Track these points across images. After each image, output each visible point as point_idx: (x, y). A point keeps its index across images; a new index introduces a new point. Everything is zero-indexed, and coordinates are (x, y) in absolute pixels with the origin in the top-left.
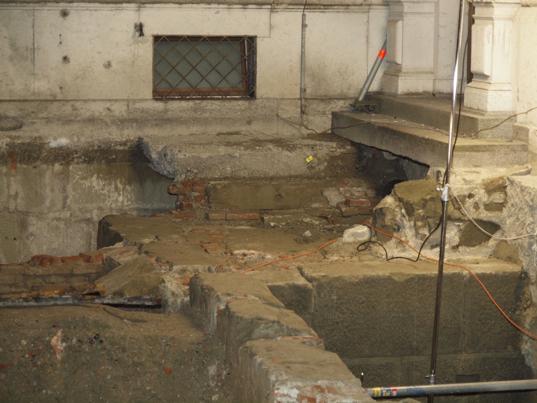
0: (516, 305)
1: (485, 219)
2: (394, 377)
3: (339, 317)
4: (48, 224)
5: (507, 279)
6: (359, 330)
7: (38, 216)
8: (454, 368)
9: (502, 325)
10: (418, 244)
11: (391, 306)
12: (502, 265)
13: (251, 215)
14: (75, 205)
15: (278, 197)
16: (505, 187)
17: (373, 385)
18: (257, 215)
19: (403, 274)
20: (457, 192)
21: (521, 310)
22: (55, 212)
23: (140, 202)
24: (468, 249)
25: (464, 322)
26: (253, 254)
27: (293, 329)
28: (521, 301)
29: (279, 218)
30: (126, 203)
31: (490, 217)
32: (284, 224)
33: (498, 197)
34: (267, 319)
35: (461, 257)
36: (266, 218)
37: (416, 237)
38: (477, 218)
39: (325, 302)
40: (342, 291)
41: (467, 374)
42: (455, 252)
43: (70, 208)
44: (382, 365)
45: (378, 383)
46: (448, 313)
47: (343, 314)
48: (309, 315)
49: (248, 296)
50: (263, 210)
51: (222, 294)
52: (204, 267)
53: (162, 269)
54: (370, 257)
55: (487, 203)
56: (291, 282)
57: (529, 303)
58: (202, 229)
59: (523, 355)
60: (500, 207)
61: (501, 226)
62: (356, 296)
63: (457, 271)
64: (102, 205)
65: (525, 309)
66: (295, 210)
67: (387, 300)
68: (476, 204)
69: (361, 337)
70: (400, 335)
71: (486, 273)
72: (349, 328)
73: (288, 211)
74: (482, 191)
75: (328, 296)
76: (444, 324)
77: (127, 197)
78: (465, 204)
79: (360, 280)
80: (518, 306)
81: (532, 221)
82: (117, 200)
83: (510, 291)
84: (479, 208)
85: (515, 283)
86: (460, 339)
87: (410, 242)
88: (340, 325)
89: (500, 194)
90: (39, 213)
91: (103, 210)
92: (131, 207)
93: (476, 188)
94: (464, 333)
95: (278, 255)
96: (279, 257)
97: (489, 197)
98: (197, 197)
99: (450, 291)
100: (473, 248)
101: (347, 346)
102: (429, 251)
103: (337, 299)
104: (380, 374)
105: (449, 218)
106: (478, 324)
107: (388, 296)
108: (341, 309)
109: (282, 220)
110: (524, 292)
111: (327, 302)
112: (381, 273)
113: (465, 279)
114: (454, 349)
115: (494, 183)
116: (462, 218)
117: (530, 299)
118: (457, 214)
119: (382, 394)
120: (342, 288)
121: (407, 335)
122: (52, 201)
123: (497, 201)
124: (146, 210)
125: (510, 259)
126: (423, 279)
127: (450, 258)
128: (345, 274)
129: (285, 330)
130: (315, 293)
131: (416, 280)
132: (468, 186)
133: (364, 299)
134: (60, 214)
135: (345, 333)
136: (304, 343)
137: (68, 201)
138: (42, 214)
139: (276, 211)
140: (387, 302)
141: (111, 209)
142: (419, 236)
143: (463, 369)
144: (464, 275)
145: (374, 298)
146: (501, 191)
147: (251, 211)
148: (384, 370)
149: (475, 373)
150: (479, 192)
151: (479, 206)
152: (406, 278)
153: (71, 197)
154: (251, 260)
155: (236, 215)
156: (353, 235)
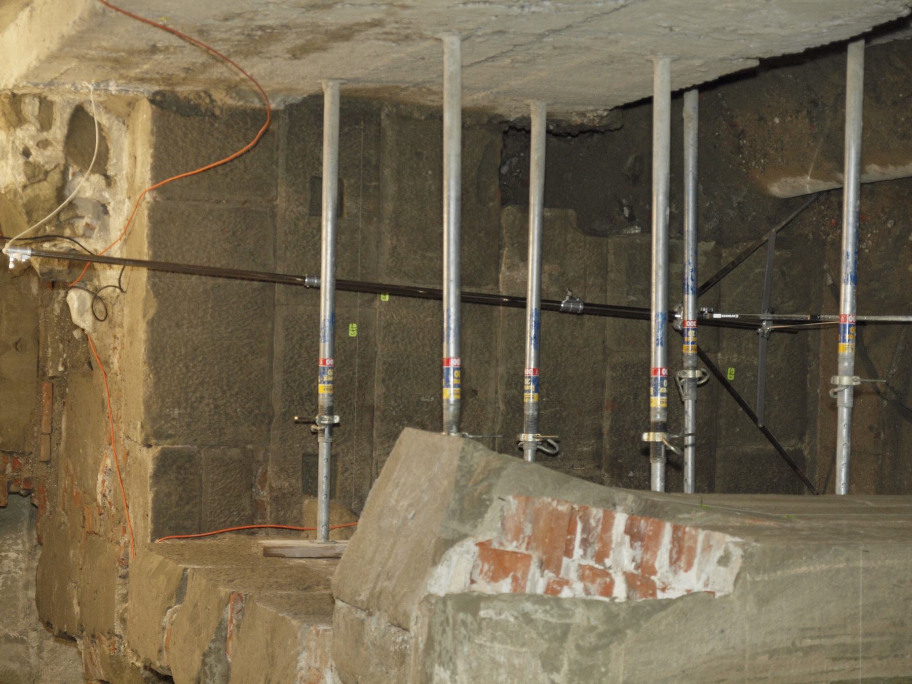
0: (206, 112)
1: (65, 131)
2: (306, 317)
3: (208, 405)
4: (47, 664)
5: (162, 129)
6: (230, 373)
7: (34, 680)
8: (298, 219)
9: (235, 139)
10: (100, 236)
11: (195, 322)
12: (140, 126)
13: (45, 395)
14: (19, 624)
15: (18, 346)
16: (14, 95)
17: (315, 351)
18: (46, 386)
19: (146, 299)
20: (19, 175)
21: (214, 107)
22: (29, 656)
23: (20, 524)
24: (113, 160)
25: (227, 201)
26: (102, 483)
27: (216, 633)
28: (200, 105)
29: (52, 353)
30: (20, 547)
31: (62, 123)
32: (61, 346)
33: (30, 108)
34: (199, 673)
35: (124, 172)
36: (51, 373)
37: (90, 237)
38: (62, 144)
39: (182, 426)
40: (167, 400)
41: (309, 196)
42: (115, 182)
43: (24, 632)
44: (286, 336)
45: (313, 342)
46: (211, 228)
47: (202, 398)
48: (202, 453)
49: (163, 624)
50: (38, 371)
51: (159, 660)
52: (119, 584)
53: (119, 648)
54: (117, 308)
55: (39, 126)
56: (149, 481)
57: (203, 95)
58: (64, 496)
59: (286, 106)
60: (46, 105)
61: (77, 103)
62: (175, 377)
63: (146, 212)
64: (21, 584)
65: (212, 101)
66: (40, 321)
67: (185, 327)
68: (40, 145)
69: (241, 369)
70: (241, 306)
71: (152, 164)
72: (225, 388)
73: (42, 334)
74: (19, 133)
75: (174, 423)
76: (227, 235)
77: (10, 546)
78: (39, 163)
79: (151, 370)
80: (207, 110)
81: (70, 85)
82: (14, 561)
83: (182, 123)
84: (46, 140)
85: (170, 116)
86: (254, 209)
87: (96, 248)
88: (220, 403)
89: (25, 103)
90: (29, 679)
91: (28, 581)
92: (26, 540)
93: (13, 142)
94: (245, 202)
95: (108, 446)
96: (110, 444)
97: (30, 122)
98: (13, 468)
99: (177, 224)
100: (111, 151)
101: (252, 392)
102: (111, 219)
103: (179, 408)
104: (300, 339)
105: (60, 193)
106: (232, 179)
107: (178, 326)
108: (195, 402)
109: (56, 349)
110: (185, 98)
111: (183, 424)
112: (142, 334)
113: (158, 199)
114: (269, 219)
115: (7, 112)
116: (62, 168)
117: (197, 93)
118: (55, 177)
119: (329, 382)
120: (163, 401)
121: (242, 295)
122: (11, 659)
123: (37, 109)
124: (32, 516)
125: (131, 104)
126: (155, 288)
127: (125, 192)
128: (142, 394)
129: (218, 645)
130: (166, 445)
131: (157, 280)
132: (10, 156)
133: (181, 365)
134: (33, 647)
135: (232, 395)
136: (238, 627)
137: (12, 634)
138: (30, 674)
139: (41, 352)
140: (188, 328)
141: (28, 569)
142: (87, 234)
143: (301, 204)
144: (152, 200)
145: (180, 348)
146: (20, 101)
147: (39, 393)
148: (294, 333)
149: (308, 185)
150: (20, 139)
151: (44, 139)
152: (153, 296)
153: (7, 631)
154: (112, 488)
155: (45, 418)
156: (81, 313)
